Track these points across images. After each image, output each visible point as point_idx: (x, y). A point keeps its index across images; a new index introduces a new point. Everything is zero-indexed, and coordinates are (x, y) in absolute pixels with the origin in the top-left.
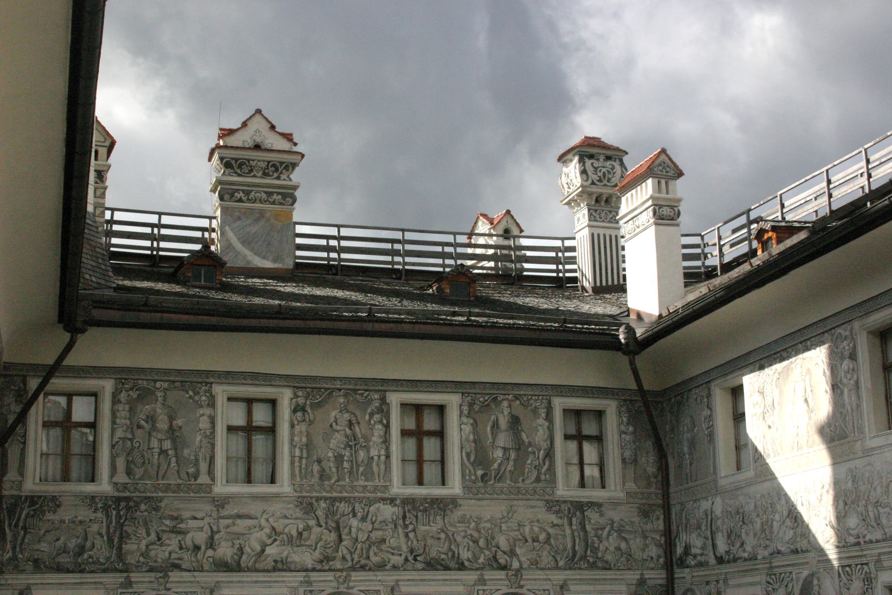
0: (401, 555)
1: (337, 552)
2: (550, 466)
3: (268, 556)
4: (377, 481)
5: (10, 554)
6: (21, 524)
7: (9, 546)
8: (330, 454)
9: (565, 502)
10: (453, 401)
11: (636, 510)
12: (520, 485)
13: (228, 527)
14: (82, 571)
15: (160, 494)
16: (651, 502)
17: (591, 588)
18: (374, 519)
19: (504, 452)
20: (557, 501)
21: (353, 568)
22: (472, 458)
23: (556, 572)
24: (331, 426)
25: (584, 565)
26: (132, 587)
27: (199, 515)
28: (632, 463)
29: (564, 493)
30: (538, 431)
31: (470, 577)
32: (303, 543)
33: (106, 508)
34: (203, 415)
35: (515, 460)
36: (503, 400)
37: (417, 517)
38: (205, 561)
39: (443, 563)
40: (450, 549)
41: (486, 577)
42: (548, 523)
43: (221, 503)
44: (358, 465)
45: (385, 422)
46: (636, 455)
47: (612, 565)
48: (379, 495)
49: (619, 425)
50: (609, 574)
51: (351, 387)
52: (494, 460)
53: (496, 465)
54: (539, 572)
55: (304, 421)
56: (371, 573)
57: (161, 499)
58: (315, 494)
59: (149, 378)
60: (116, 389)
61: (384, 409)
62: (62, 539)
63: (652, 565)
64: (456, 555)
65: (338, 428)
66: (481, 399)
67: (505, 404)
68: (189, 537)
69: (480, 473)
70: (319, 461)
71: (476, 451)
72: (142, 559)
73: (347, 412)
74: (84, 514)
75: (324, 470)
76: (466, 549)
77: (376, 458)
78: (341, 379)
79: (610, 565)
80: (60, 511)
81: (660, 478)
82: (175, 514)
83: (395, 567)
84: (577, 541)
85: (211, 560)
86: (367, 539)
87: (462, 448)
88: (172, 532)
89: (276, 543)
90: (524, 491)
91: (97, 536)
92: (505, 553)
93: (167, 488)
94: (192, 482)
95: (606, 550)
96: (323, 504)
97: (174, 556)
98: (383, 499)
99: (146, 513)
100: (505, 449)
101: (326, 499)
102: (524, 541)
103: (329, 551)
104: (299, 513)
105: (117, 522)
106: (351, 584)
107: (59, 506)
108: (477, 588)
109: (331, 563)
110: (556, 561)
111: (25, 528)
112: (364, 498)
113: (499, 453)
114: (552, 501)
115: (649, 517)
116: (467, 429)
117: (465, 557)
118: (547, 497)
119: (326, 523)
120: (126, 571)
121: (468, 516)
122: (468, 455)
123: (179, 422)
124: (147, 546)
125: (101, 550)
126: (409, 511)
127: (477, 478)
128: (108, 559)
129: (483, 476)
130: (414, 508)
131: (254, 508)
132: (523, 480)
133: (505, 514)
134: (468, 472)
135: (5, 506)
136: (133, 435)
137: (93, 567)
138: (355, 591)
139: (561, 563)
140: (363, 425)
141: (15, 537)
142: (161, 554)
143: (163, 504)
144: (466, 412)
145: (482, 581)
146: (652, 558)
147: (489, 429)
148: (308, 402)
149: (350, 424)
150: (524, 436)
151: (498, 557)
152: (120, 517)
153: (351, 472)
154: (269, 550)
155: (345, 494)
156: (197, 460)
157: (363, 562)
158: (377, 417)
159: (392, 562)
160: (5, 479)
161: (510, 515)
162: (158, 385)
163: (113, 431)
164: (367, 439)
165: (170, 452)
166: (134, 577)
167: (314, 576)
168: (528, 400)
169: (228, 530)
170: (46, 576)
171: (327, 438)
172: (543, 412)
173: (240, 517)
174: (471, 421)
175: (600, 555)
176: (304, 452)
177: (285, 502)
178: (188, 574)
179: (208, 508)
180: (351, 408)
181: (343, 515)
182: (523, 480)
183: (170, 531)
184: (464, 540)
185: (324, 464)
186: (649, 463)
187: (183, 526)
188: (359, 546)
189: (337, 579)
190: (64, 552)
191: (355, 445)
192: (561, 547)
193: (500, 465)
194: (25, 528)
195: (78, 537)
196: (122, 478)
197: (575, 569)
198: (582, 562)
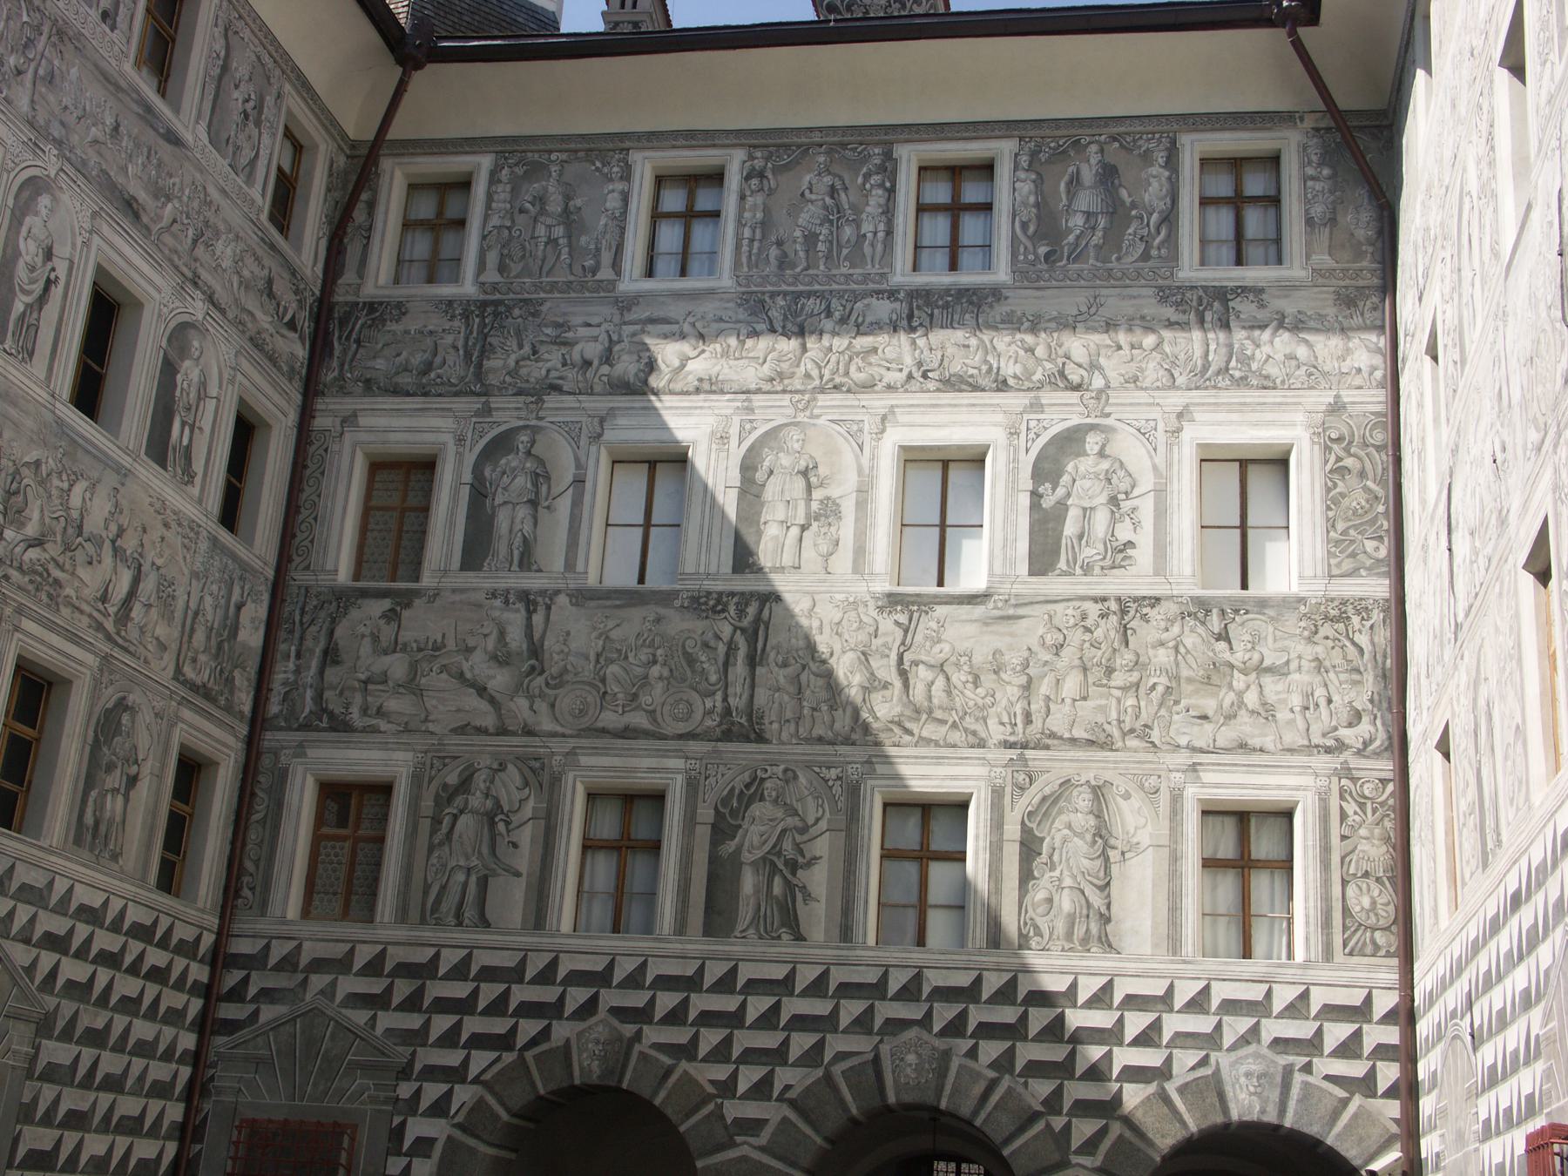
0: (901, 370)
1: (798, 366)
2: (1169, 236)
3: (690, 373)
4: (869, 266)
5: (336, 373)
6: (354, 336)
7: (335, 363)
8: (798, 233)
9: (1192, 288)
10: (1004, 150)
11: (1332, 296)
12: (1114, 264)
13: (634, 335)
14: (425, 394)
15: (542, 295)
16: (1361, 283)
17: (1235, 417)
18: (860, 319)
19: (1087, 220)
20: (1179, 288)
21: (822, 390)
22: (1032, 229)
23: (1172, 393)
24: (803, 195)
25: (1223, 382)
26: (491, 416)
27: (595, 320)
28: (1325, 225)
29: (1192, 274)
30: (1150, 185)
31: (1015, 401)
32: (744, 354)
33: (466, 316)
34: (613, 191)
36: (1090, 143)
37: (931, 316)
38: (596, 380)
39: (970, 380)
40: (986, 362)
41: (1043, 401)
42: (1160, 321)
43: (626, 304)
44: (840, 247)
45: (888, 185)
46: (1334, 211)
47: (1278, 381)
48: (871, 286)
49: (1303, 166)
50: (1271, 396)
51: (836, 139)
52: (1069, 231)
53: (1071, 238)
54: (1142, 393)
55: (762, 189)
56: (851, 396)
57: (542, 302)
58: (770, 288)
59: (542, 147)
60: (496, 165)
61: (888, 168)
62: (405, 354)
63: (1358, 381)
65: (813, 197)
66: (1052, 145)
67: (1094, 148)
68: (578, 348)
69: (1043, 250)
70: (779, 243)
71: (1038, 217)
72: (508, 379)
73: (830, 174)
74: (436, 322)
75: (785, 255)
76: (1012, 361)
77: (869, 235)
78: (820, 129)
79: (1274, 381)
80: (405, 319)
81: (1379, 245)
82: (561, 320)
83: (889, 387)
84: (1212, 347)
85: (605, 379)
86: (847, 348)
87: (1014, 216)
88: (555, 343)
89: (703, 356)
90: (1119, 274)
91: (451, 351)
92: (1080, 366)
93: (553, 287)
94: (589, 277)
95: (1266, 361)
96: (781, 302)
97: (553, 374)
98: (878, 292)
99: (520, 320)
100: (1088, 215)
101: (785, 294)
103: (785, 366)
104: (742, 315)
105: (480, 332)
106: (816, 411)
107: (404, 314)
108: (1026, 417)
109: (786, 382)
110: (1172, 375)
111: (358, 341)
112: (846, 291)
113: (1079, 220)
114: (1169, 288)
115: (1356, 306)
116: (1026, 188)
117: (1010, 371)
119: (784, 327)
120: (485, 395)
122: (1024, 226)
123: (578, 202)
124: (517, 362)
125: (453, 368)
126: (919, 308)
128: (462, 379)
129: (1047, 256)
130: (928, 304)
131: (675, 310)
132: (1119, 259)
133: (1083, 309)
134: (1022, 250)
135: (336, 315)
136: (513, 221)
137: (441, 390)
138: (821, 421)
139: (1180, 380)
140: (851, 192)
141: (345, 352)
142: (535, 372)
143: (544, 308)
144: (1025, 165)
145: (1036, 407)
146: (1359, 370)
147: (1062, 186)
148: (769, 165)
149: (833, 191)
150: (1124, 193)
152: (485, 325)
153: (828, 257)
154: (691, 366)
155: (817, 287)
156: (598, 250)
157: (838, 380)
158: (875, 179)
159: (885, 380)
160: (340, 282)
161: (1093, 310)
162: (553, 157)
163: (486, 218)
164: (857, 210)
165: (561, 241)
166: (496, 402)
167: (758, 400)
168: (1134, 141)
169: (635, 339)
170: (380, 399)
171: (794, 211)
172: (1160, 158)
173: (652, 321)
174: (1033, 176)
175: (1254, 366)
176: (758, 231)
177: (722, 299)
178: (571, 398)
179: (607, 311)
180: (836, 169)
181: (812, 315)
182: (1119, 259)
183: (551, 343)
185: (785, 247)
186: (1359, 222)
187: (570, 335)
188: (834, 359)
189: (794, 405)
190: (406, 370)
191: (838, 219)
192: (1182, 356)
193: (1078, 237)
194: (358, 341)
195: (425, 351)
196: (492, 276)
197: (1206, 388)
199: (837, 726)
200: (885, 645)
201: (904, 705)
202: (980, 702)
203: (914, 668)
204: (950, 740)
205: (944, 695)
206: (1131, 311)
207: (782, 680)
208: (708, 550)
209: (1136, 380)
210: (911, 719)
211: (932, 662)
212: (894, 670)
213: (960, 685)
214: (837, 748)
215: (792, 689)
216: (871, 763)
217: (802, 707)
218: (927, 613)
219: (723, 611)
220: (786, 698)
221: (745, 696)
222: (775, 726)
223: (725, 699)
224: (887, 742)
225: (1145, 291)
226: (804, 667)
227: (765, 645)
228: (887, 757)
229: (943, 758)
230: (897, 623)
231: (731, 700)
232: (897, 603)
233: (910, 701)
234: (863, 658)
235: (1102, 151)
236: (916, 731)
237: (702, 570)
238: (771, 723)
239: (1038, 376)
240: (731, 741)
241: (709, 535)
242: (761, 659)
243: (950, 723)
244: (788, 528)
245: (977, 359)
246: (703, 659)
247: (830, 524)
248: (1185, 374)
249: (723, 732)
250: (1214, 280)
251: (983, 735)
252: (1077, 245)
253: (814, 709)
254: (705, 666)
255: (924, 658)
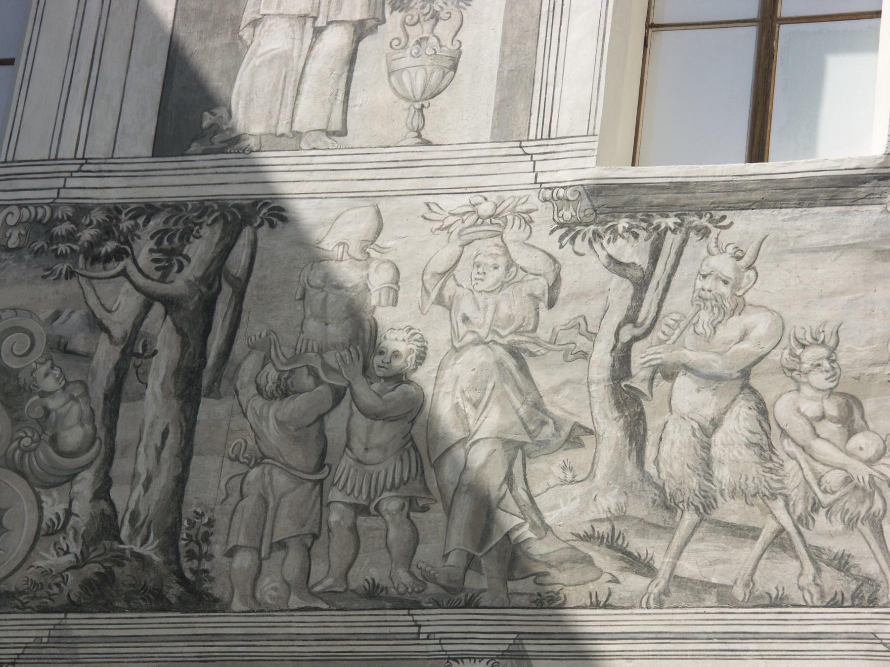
199: (426, 553)
200: (581, 326)
201: (627, 490)
202: (862, 472)
203: (662, 385)
204: (766, 584)
205: (749, 456)
207: (272, 432)
208: (90, 98)
210: (645, 527)
211: (718, 365)
212: (601, 392)
213: (799, 429)
214: (420, 616)
215: (299, 457)
216: (523, 656)
217: (324, 505)
218: (704, 233)
219: (118, 254)
220: (281, 480)
221: (162, 482)
222: (244, 560)
223: (102, 492)
224: (574, 595)
226: (338, 395)
227: (230, 340)
228: (573, 637)
229: (745, 637)
230: (616, 265)
231: (118, 494)
232: (615, 212)
233: (646, 478)
234: (511, 363)
236: (662, 562)
237: (66, 151)
238: (231, 553)
240: (108, 607)
241: (98, 59)
242: (217, 379)
243: (766, 535)
244: (318, 32)
246: (50, 384)
247: (436, 17)
249: (87, 585)
251: (871, 568)
253: (360, 510)
254: (53, 404)
255: (691, 356)
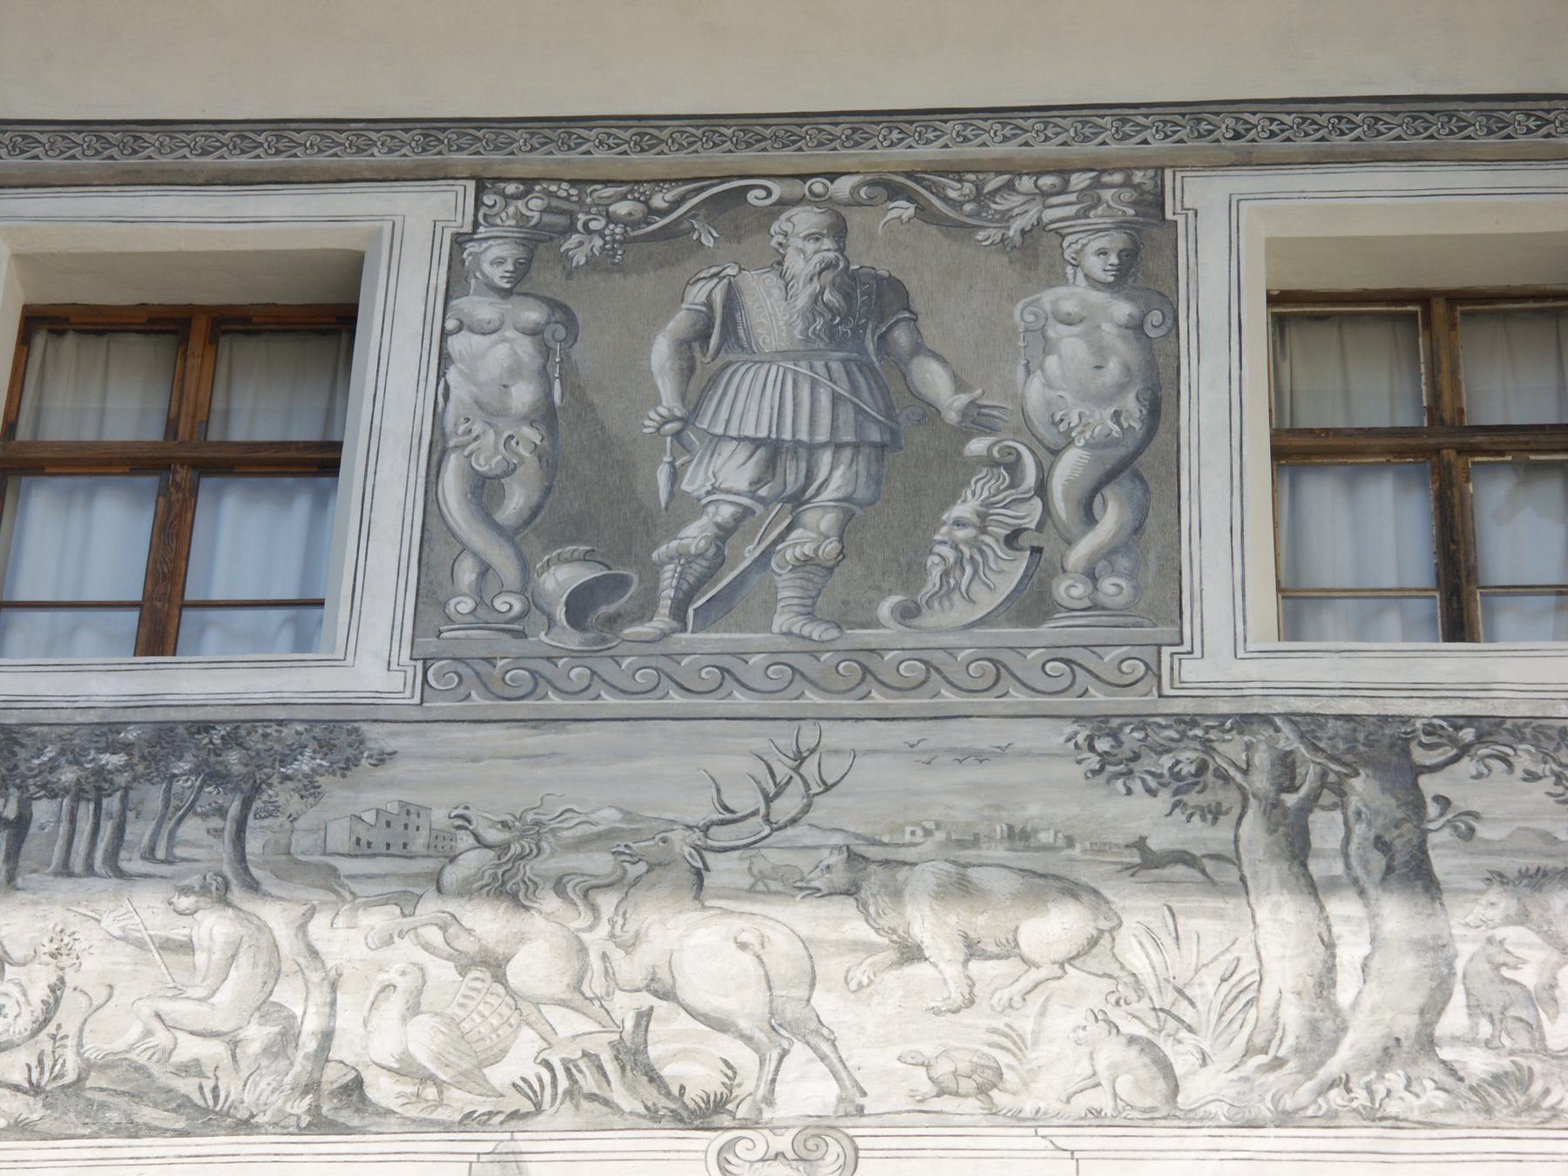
19: (771, 466)
22: (516, 501)
30: (1048, 347)
35: (847, 504)
36: (784, 204)
39: (187, 1086)
40: (265, 1008)
42: (1100, 848)
52: (686, 508)
53: (695, 535)
64: (309, 1044)
66: (621, 209)
71: (550, 462)
76: (394, 1005)
90: (911, 670)
92: (720, 1025)
100: (772, 452)
102: (892, 955)
110: (1165, 1067)
114: (1142, 721)
117: (384, 1048)
118: (1100, 700)
121: (440, 817)
122: (484, 490)
127: (533, 602)
129: (580, 605)
133: (744, 799)
134: (467, 574)
139: (1199, 1087)
144: (498, 276)
147: (661, 351)
150: (934, 379)
151: (654, 1052)
161: (787, 806)
168: (979, 196)
174: (533, 314)
182: (907, 613)
184: (386, 954)
192: (1207, 989)
193: (724, 533)
197: (1330, 1120)
198: (1395, 1078)
206: (964, 810)
209: (987, 1083)
225: (1026, 734)
235: (839, 230)
239: (519, 1063)
245: (225, 995)
248: (1222, 1059)
250: (1350, 691)
252: (718, 562)
